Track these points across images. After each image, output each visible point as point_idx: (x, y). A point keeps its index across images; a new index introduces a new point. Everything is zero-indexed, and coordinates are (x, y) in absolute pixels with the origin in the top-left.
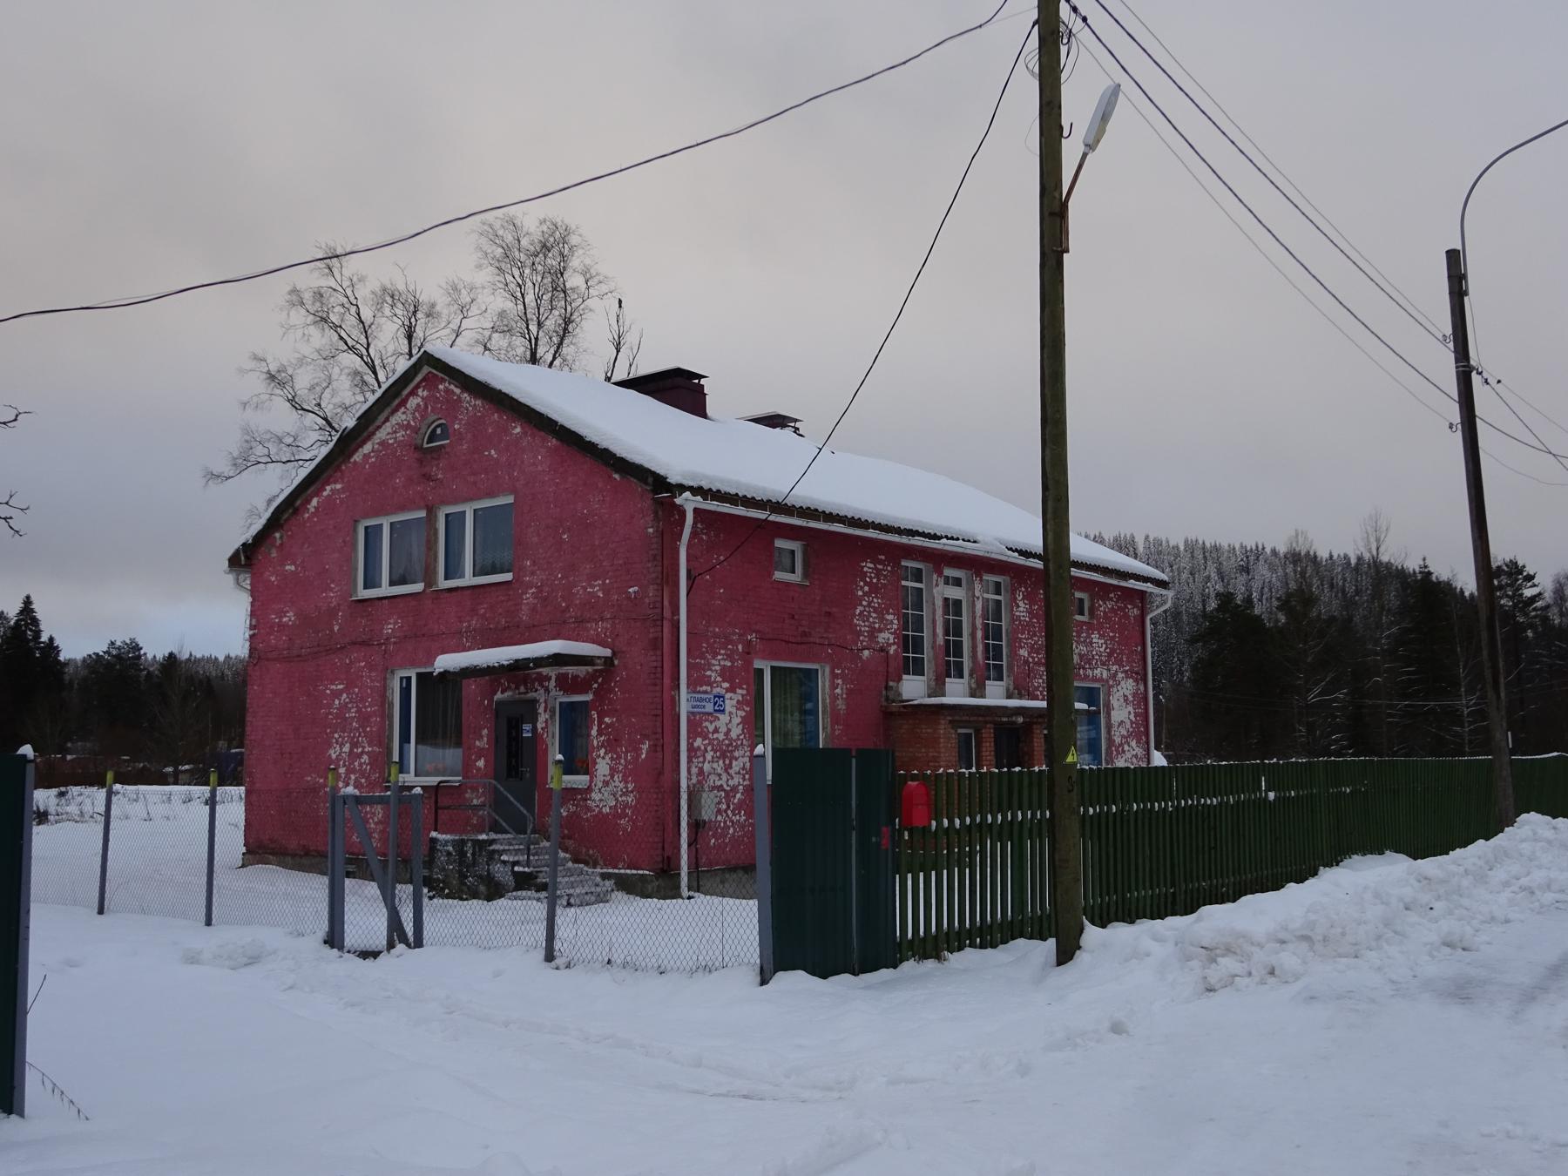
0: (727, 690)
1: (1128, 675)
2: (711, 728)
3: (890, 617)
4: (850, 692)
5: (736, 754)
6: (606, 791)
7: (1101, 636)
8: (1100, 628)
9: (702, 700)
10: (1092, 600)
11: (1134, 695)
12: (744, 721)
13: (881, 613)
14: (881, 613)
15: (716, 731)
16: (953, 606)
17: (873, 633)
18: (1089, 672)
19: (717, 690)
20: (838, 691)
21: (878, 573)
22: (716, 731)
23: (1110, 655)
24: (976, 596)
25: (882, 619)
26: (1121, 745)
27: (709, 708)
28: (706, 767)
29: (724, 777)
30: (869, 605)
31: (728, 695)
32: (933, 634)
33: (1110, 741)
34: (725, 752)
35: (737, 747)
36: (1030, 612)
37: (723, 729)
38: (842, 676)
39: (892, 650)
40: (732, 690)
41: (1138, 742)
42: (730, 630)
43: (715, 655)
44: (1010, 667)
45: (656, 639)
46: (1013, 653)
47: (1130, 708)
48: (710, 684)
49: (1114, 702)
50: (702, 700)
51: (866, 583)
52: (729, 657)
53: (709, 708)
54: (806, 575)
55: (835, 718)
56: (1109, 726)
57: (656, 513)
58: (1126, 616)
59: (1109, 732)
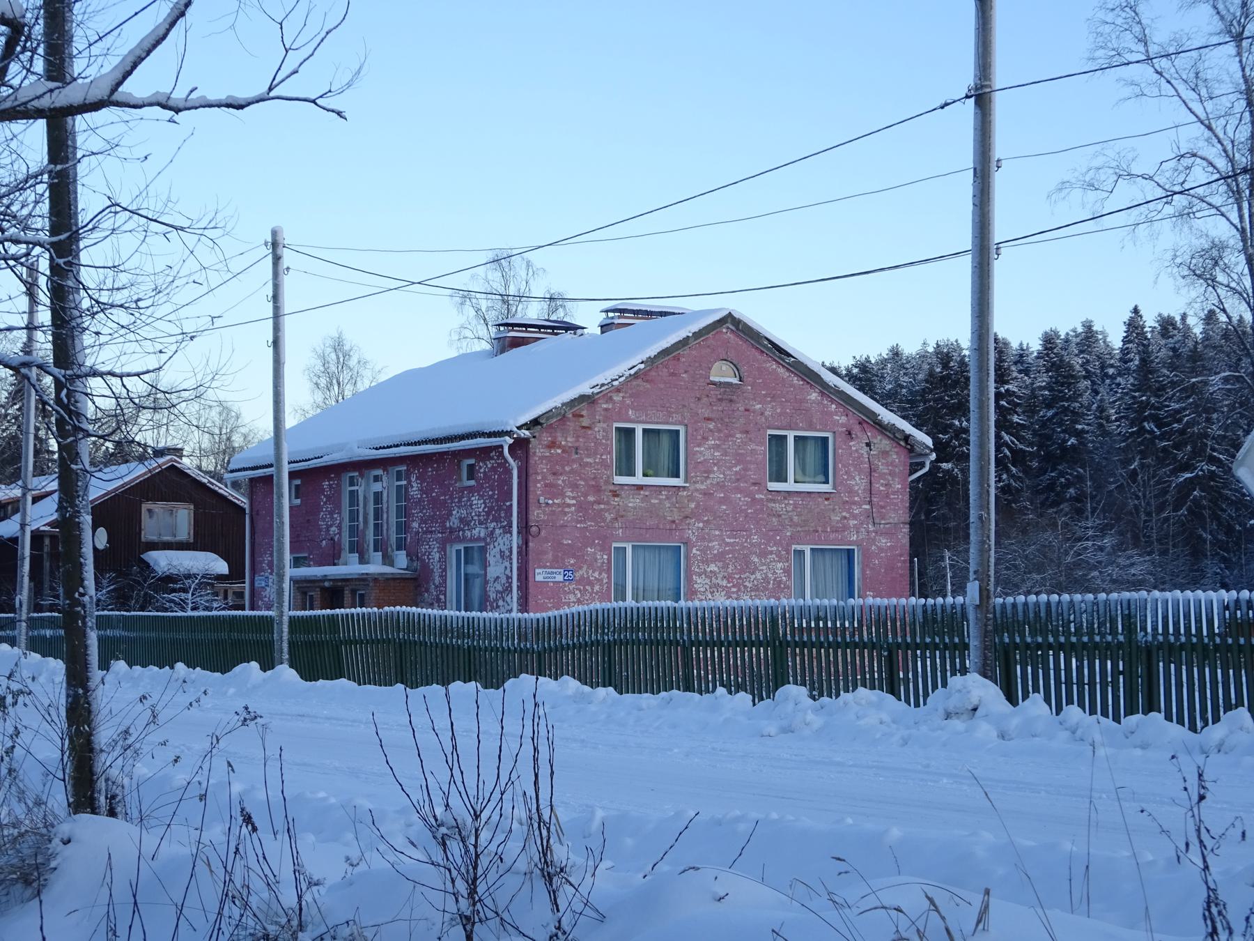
7: (481, 497)
13: (331, 513)
16: (378, 497)
17: (328, 527)
18: (468, 534)
23: (488, 514)
24: (385, 485)
25: (332, 518)
26: (496, 600)
36: (421, 490)
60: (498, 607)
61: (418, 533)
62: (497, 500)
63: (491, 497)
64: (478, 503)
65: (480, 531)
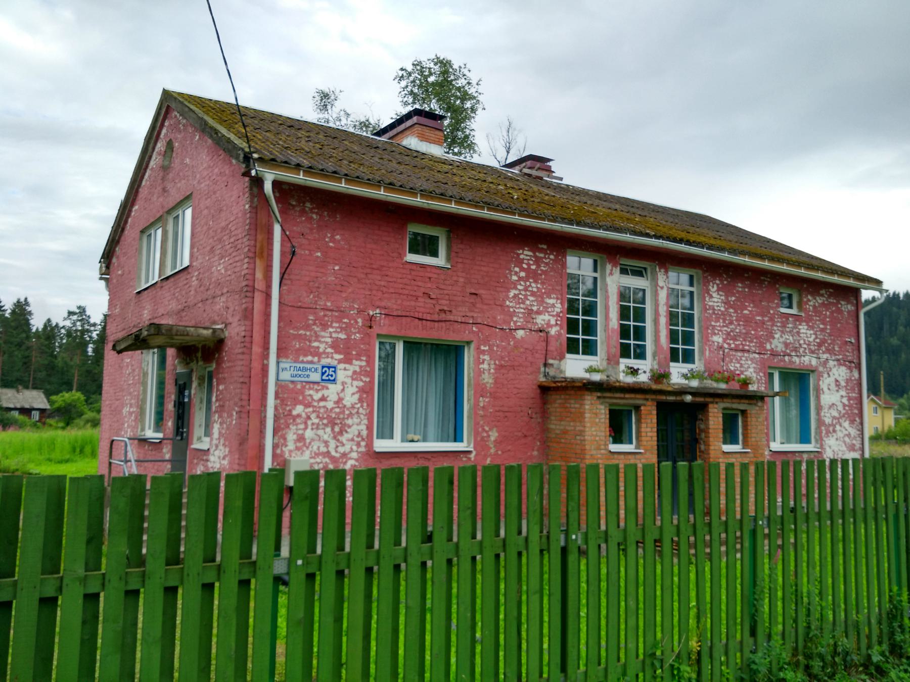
0: (340, 361)
1: (840, 363)
2: (317, 396)
3: (551, 301)
4: (499, 368)
5: (350, 422)
6: (217, 453)
7: (811, 328)
8: (808, 320)
9: (306, 369)
10: (800, 295)
11: (848, 381)
12: (361, 390)
14: (540, 297)
15: (324, 399)
17: (530, 314)
19: (325, 361)
20: (485, 366)
21: (538, 261)
22: (324, 399)
23: (819, 345)
27: (316, 377)
28: (309, 434)
29: (332, 444)
30: (526, 289)
31: (342, 366)
32: (608, 319)
33: (820, 422)
34: (336, 422)
35: (351, 415)
36: (726, 303)
37: (333, 397)
38: (490, 352)
39: (553, 331)
40: (348, 360)
41: (852, 422)
42: (345, 304)
43: (325, 327)
44: (702, 352)
45: (246, 309)
46: (705, 339)
47: (843, 393)
48: (317, 353)
49: (824, 385)
50: (306, 369)
51: (522, 269)
52: (345, 329)
53: (316, 377)
54: (448, 259)
55: (480, 390)
56: (819, 408)
57: (251, 189)
58: (839, 311)
59: (818, 414)
60: (834, 431)
61: (721, 347)
62: (830, 335)
63: (822, 330)
64: (806, 333)
65: (809, 360)
